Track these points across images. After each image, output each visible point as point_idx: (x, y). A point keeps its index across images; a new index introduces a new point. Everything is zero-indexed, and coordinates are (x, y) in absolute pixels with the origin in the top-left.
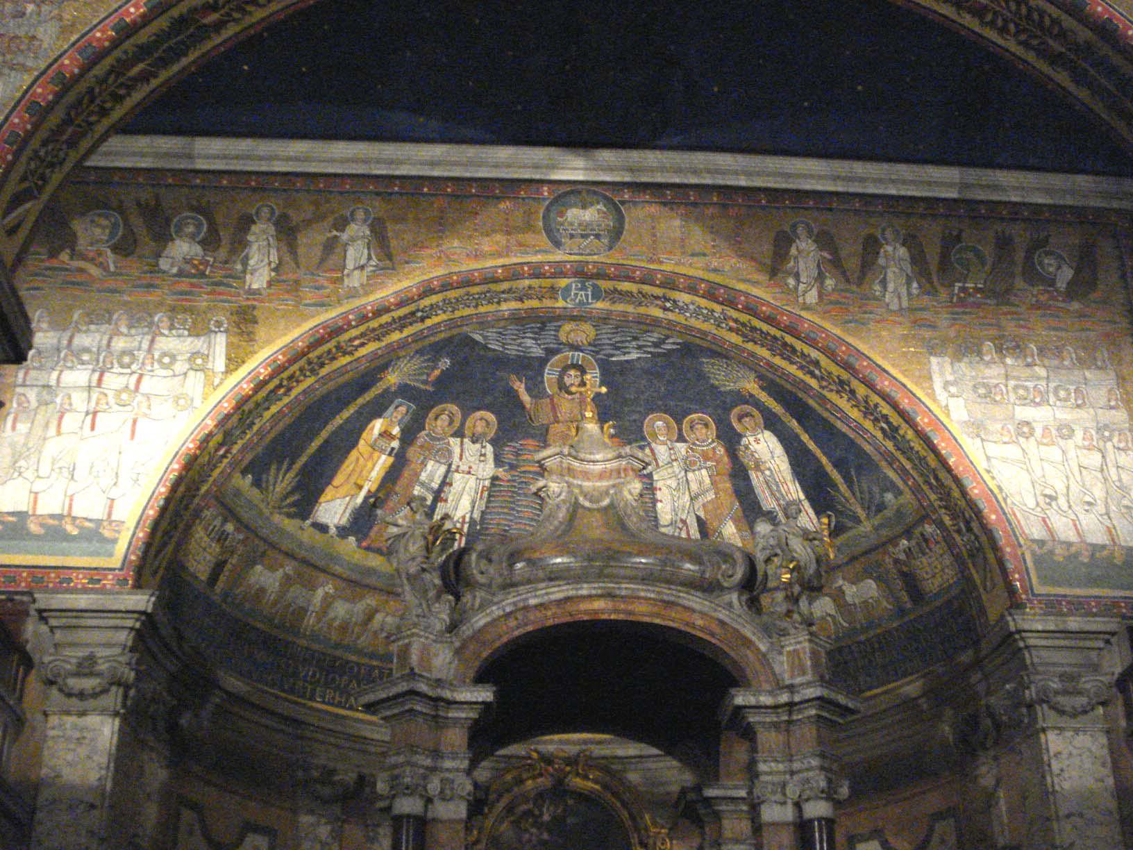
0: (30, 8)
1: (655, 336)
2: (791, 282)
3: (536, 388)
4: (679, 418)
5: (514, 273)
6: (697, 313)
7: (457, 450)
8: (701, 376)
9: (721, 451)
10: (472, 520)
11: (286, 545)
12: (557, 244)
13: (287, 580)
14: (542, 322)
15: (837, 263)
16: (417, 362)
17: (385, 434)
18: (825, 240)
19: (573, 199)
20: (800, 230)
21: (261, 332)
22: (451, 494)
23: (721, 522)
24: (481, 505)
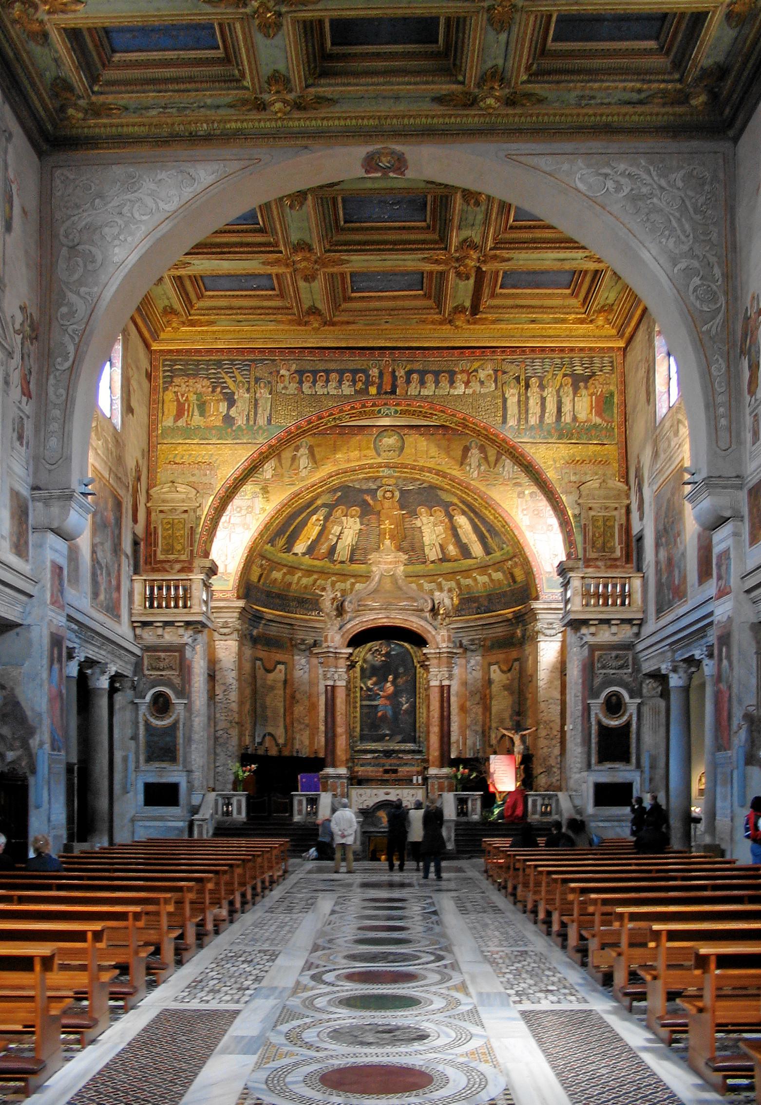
0: (208, 472)
1: (419, 483)
2: (468, 468)
3: (374, 497)
4: (431, 508)
5: (362, 468)
6: (433, 478)
7: (345, 522)
8: (437, 495)
9: (447, 520)
10: (353, 545)
11: (285, 563)
12: (379, 455)
13: (285, 574)
14: (376, 479)
15: (486, 458)
16: (328, 495)
17: (318, 520)
18: (482, 449)
19: (385, 434)
20: (473, 445)
21: (272, 498)
22: (343, 536)
23: (448, 544)
24: (356, 539)
